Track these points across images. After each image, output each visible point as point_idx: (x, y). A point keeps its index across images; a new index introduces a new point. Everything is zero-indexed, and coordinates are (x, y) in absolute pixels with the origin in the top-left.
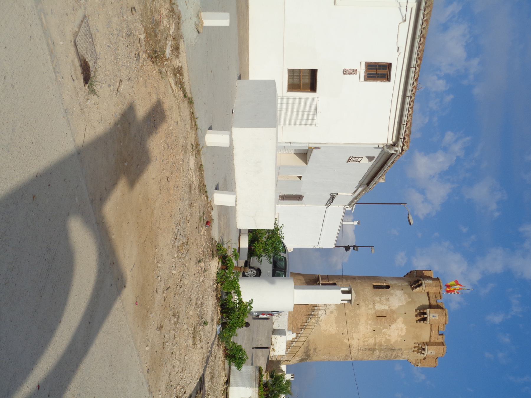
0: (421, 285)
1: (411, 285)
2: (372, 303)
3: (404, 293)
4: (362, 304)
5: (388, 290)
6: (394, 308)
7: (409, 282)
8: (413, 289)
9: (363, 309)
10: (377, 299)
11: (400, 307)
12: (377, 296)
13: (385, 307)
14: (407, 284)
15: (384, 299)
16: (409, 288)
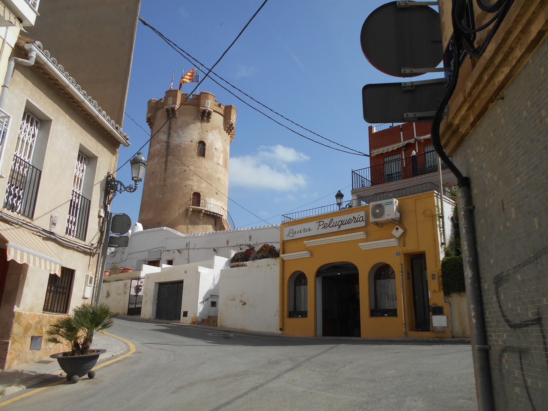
0: (209, 113)
1: (202, 120)
2: (219, 166)
3: (211, 132)
4: (218, 175)
5: (207, 144)
6: (223, 149)
7: (195, 119)
8: (208, 121)
9: (222, 177)
10: (215, 159)
11: (222, 143)
12: (213, 158)
13: (222, 155)
14: (199, 124)
15: (215, 153)
16: (205, 124)
